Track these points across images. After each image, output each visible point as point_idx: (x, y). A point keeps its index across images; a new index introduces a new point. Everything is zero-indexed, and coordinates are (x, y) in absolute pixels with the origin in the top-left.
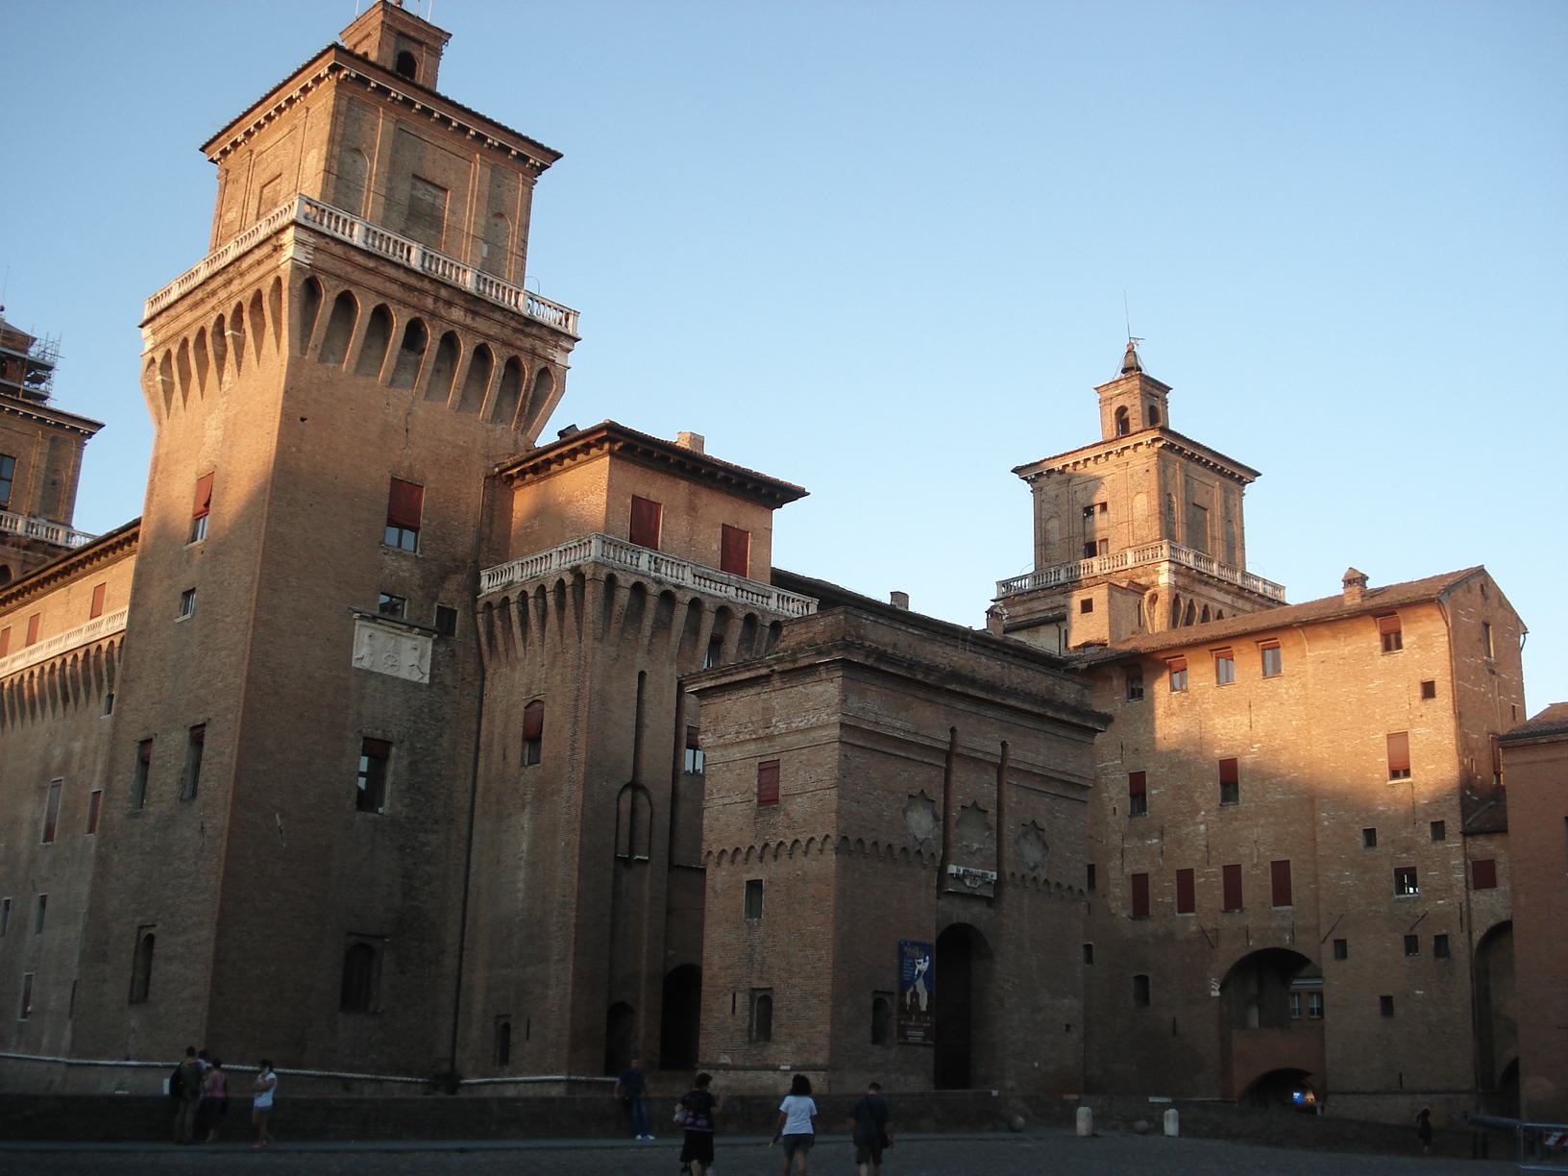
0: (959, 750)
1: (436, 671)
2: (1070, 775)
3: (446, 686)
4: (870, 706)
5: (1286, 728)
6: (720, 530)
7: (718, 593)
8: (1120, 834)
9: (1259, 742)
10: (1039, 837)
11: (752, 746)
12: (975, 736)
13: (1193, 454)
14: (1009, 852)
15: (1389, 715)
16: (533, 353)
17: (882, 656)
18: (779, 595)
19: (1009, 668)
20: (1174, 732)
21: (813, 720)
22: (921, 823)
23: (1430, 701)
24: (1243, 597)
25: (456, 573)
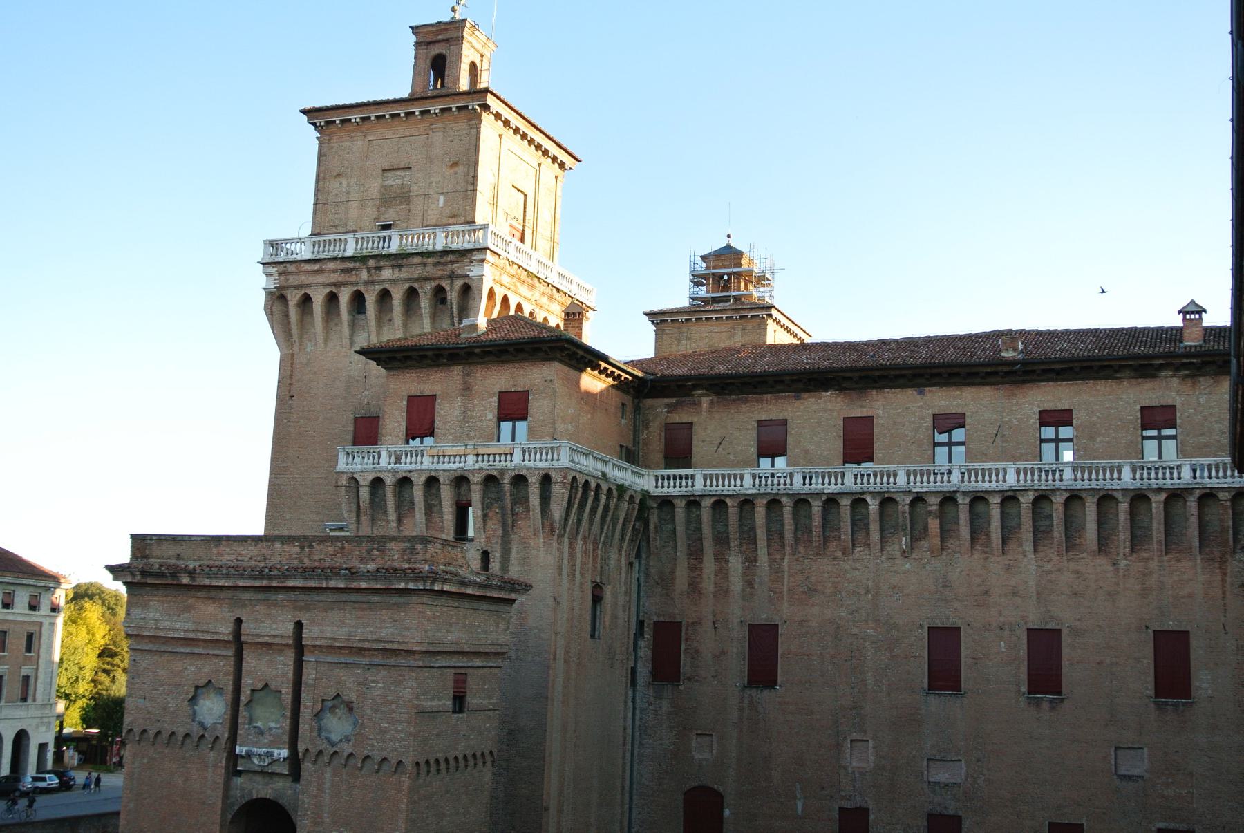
2: (385, 642)
4: (152, 615)
6: (496, 399)
12: (262, 622)
14: (304, 728)
16: (452, 276)
22: (213, 709)
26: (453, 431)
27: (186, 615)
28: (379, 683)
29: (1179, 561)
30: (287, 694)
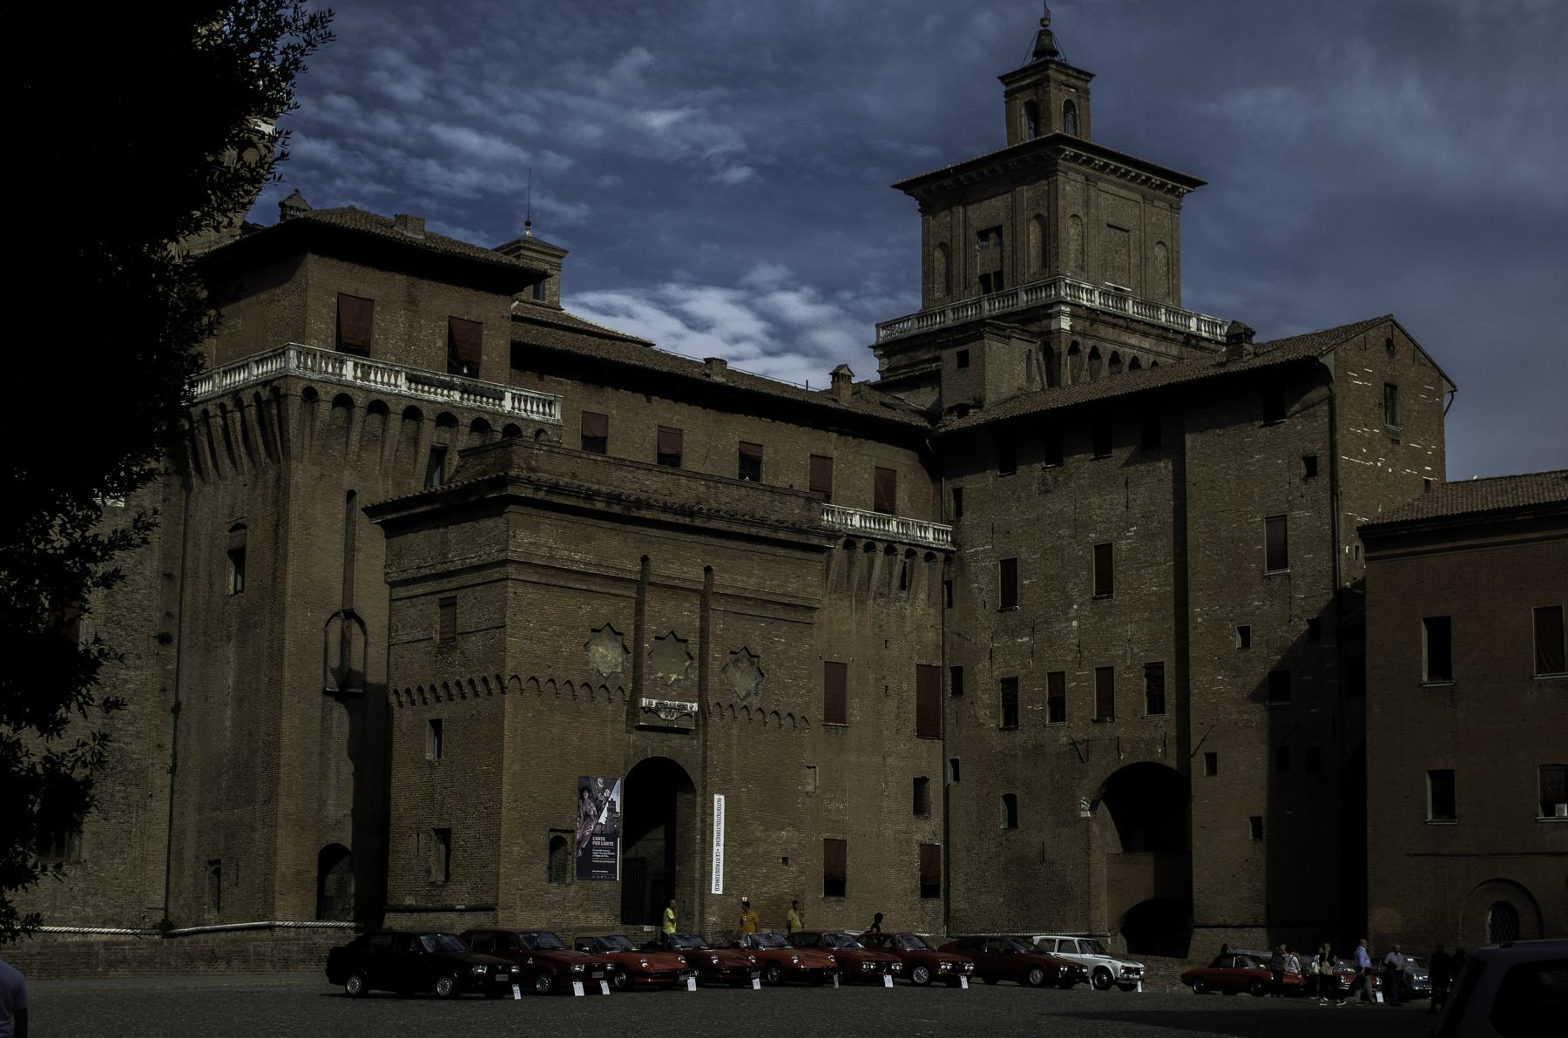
0: (652, 579)
4: (543, 541)
6: (445, 323)
7: (440, 399)
10: (753, 663)
11: (432, 586)
13: (1106, 165)
14: (713, 680)
15: (1269, 495)
17: (554, 488)
18: (514, 395)
19: (716, 488)
20: (1048, 512)
21: (485, 557)
22: (607, 657)
24: (1166, 339)
26: (396, 352)
27: (585, 545)
28: (781, 637)
29: (841, 600)
30: (695, 643)
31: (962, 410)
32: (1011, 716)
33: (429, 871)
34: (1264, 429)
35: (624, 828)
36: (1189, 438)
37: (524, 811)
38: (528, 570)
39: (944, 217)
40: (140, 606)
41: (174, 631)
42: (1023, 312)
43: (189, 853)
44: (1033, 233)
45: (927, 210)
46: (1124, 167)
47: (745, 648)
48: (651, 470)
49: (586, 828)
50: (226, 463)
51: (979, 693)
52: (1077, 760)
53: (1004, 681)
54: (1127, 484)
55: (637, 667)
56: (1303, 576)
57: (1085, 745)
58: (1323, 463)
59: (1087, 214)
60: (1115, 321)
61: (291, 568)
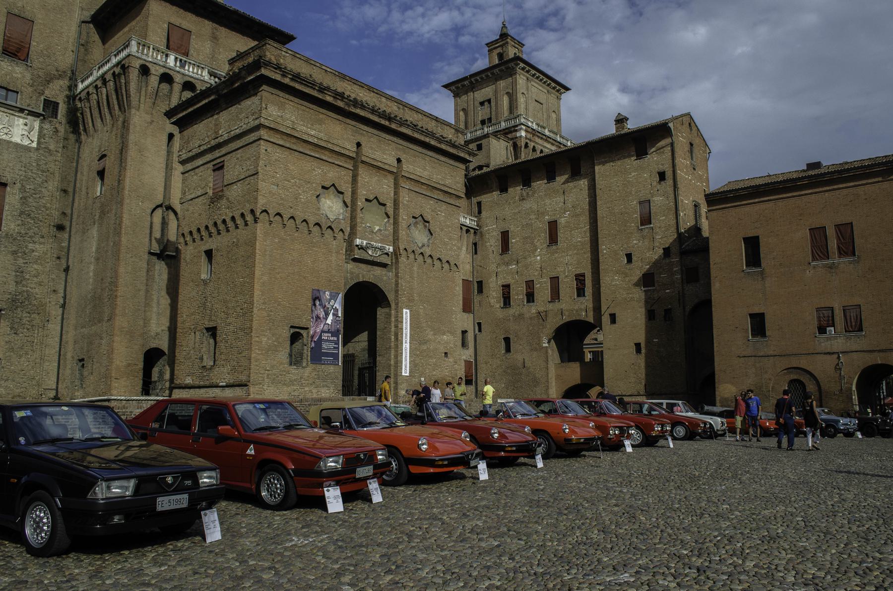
0: (364, 159)
1: (42, 140)
3: (50, 150)
4: (288, 116)
5: (584, 203)
8: (495, 264)
9: (569, 211)
10: (425, 226)
11: (209, 157)
12: (375, 151)
13: (535, 74)
14: (402, 233)
15: (640, 191)
17: (296, 77)
19: (403, 109)
22: (332, 207)
23: (662, 182)
25: (58, 79)
28: (442, 212)
31: (480, 168)
32: (507, 300)
33: (202, 359)
34: (636, 161)
35: (344, 328)
36: (597, 168)
37: (271, 311)
38: (276, 136)
39: (464, 98)
40: (44, 207)
41: (67, 224)
42: (504, 130)
43: (69, 355)
44: (506, 100)
45: (456, 95)
46: (542, 77)
47: (421, 215)
48: (363, 87)
49: (317, 326)
50: (98, 121)
51: (491, 292)
52: (541, 320)
53: (503, 286)
54: (564, 193)
55: (353, 218)
56: (660, 227)
57: (544, 313)
58: (669, 174)
59: (528, 93)
60: (542, 136)
61: (129, 174)
